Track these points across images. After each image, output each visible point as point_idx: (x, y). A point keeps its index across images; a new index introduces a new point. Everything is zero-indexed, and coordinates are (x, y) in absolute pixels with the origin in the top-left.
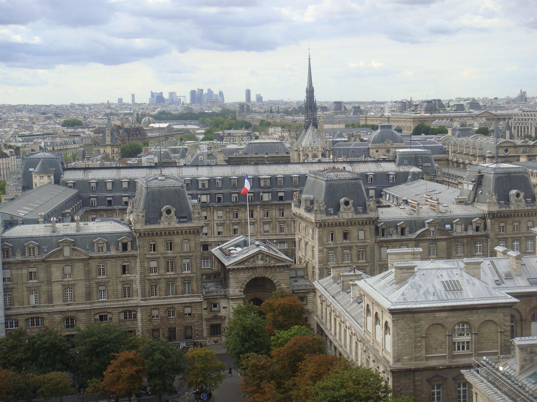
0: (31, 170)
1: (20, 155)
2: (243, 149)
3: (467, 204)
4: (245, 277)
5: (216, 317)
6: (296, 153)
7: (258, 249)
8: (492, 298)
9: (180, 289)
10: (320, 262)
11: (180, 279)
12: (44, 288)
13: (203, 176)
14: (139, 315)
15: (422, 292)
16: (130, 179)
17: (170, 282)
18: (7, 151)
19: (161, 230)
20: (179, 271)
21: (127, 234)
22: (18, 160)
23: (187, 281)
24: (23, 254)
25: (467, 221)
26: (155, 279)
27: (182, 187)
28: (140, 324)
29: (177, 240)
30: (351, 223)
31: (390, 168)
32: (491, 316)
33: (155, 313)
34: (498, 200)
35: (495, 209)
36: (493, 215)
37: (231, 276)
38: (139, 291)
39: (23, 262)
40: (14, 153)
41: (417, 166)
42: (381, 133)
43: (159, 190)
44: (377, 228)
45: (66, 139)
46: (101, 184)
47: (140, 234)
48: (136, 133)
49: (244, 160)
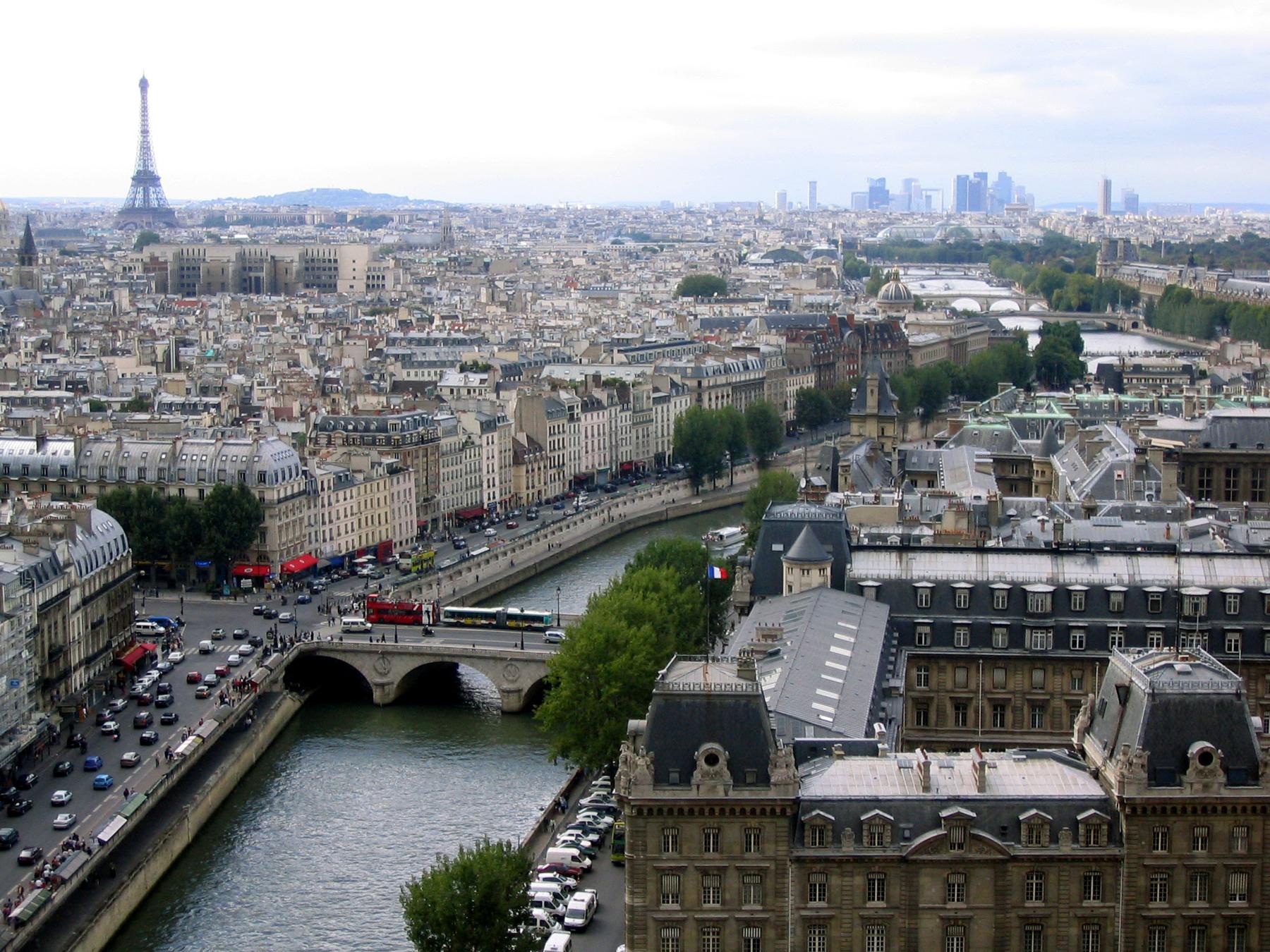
0: (777, 547)
1: (628, 402)
2: (1199, 431)
11: (1219, 921)
12: (900, 922)
13: (1193, 584)
16: (1012, 583)
18: (600, 394)
19: (1184, 802)
21: (1096, 804)
22: (623, 414)
24: (859, 840)
26: (1160, 918)
27: (1238, 695)
29: (1221, 825)
39: (858, 860)
40: (616, 399)
43: (1181, 702)
45: (728, 360)
46: (943, 592)
47: (1134, 810)
48: (882, 336)
49: (1201, 459)
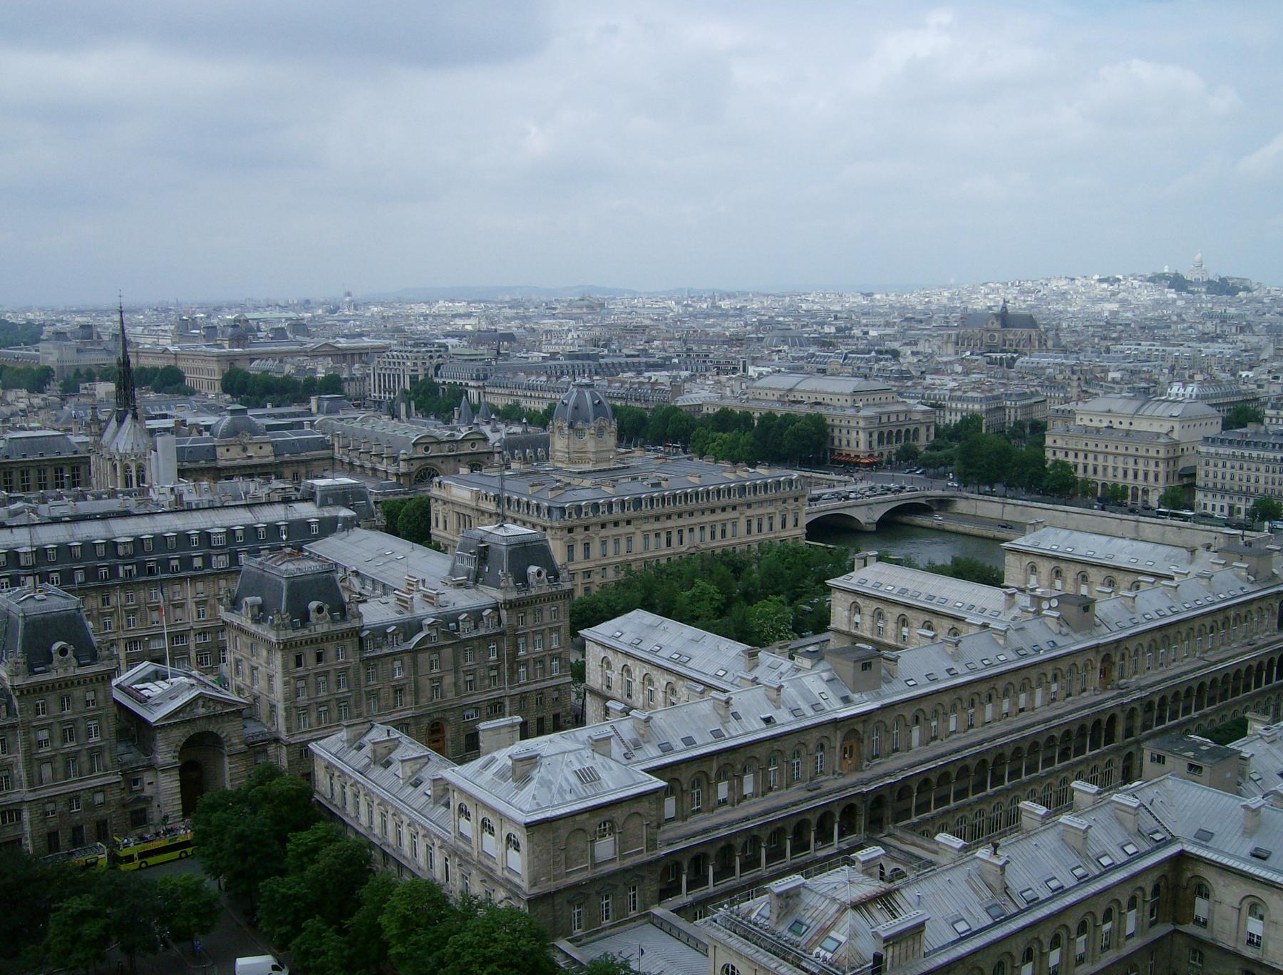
3: (468, 588)
4: (179, 736)
5: (139, 800)
6: (109, 463)
7: (194, 693)
8: (636, 784)
9: (86, 766)
10: (286, 700)
14: (26, 815)
15: (555, 789)
17: (70, 758)
20: (83, 740)
23: (95, 753)
25: (476, 616)
28: (27, 828)
29: (77, 693)
30: (327, 637)
31: (307, 511)
32: (637, 807)
33: (50, 807)
34: (515, 583)
35: (513, 595)
36: (510, 605)
37: (159, 736)
38: (24, 778)
41: (348, 507)
42: (232, 422)
44: (361, 640)
